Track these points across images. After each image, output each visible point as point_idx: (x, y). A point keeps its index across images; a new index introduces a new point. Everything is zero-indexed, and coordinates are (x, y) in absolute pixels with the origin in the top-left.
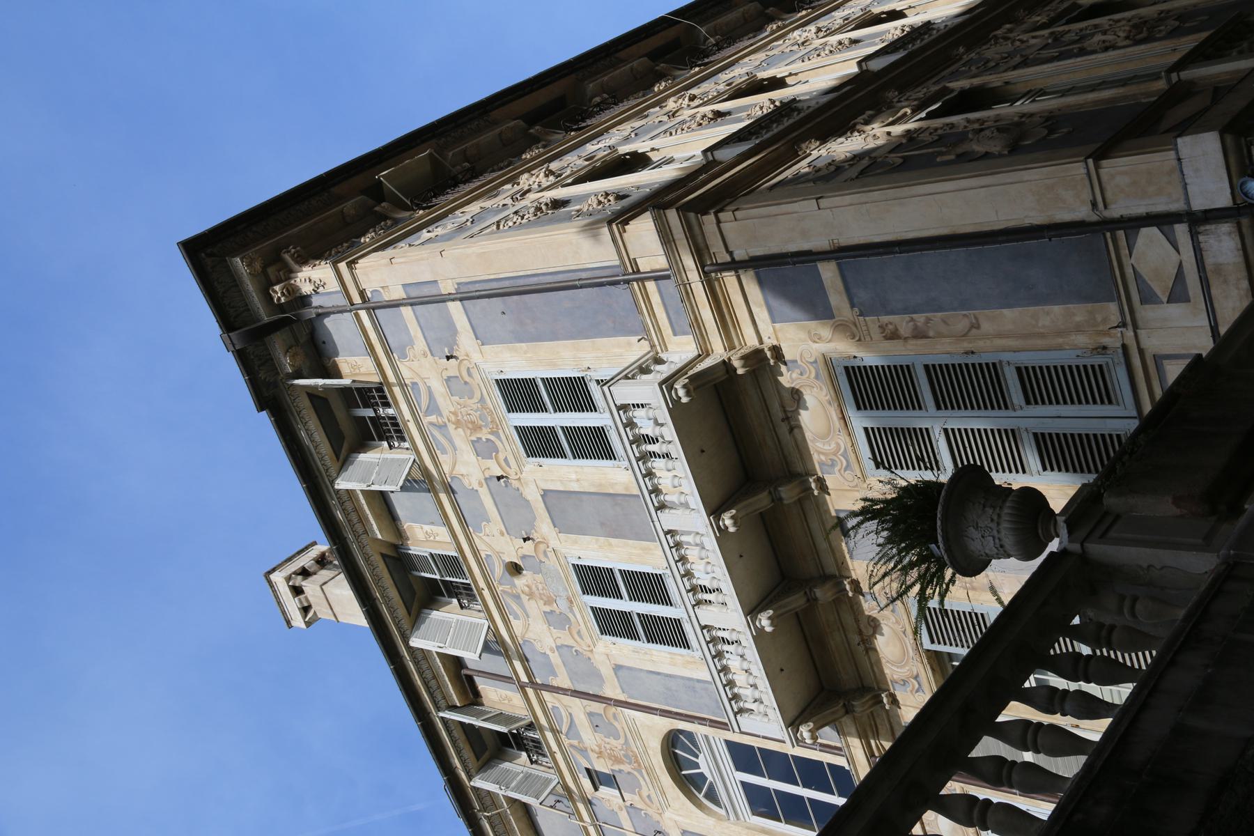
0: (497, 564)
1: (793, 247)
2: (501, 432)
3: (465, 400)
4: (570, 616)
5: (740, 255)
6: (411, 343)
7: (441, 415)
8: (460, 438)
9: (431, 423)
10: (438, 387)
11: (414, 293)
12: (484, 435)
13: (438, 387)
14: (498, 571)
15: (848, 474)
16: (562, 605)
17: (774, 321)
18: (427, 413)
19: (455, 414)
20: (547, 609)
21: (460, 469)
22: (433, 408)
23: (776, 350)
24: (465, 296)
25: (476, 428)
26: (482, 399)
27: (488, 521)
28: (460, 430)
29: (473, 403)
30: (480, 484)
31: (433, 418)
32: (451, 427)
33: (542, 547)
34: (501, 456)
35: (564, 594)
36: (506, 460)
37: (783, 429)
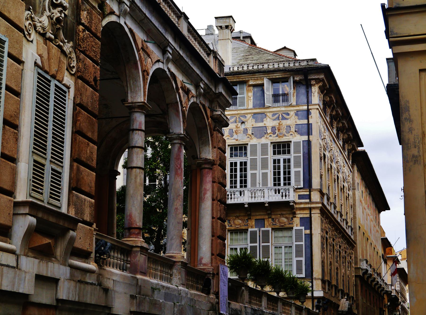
0: (244, 119)
1: (313, 226)
2: (277, 138)
3: (285, 131)
4: (233, 138)
5: (312, 215)
6: (299, 119)
7: (282, 120)
8: (275, 123)
9: (279, 115)
10: (288, 122)
11: (310, 126)
12: (277, 131)
13: (288, 122)
14: (243, 119)
15: (272, 224)
16: (235, 136)
17: (300, 218)
18: (282, 116)
19: (282, 125)
20: (234, 131)
21: (268, 119)
22: (284, 118)
23: (295, 217)
24: (309, 142)
25: (279, 130)
26: (285, 136)
27: (256, 122)
28: (278, 124)
29: (284, 132)
30: (265, 124)
31: (281, 116)
32: (278, 121)
33: (250, 137)
34: (272, 135)
35: (239, 138)
36: (271, 136)
37: (280, 213)
